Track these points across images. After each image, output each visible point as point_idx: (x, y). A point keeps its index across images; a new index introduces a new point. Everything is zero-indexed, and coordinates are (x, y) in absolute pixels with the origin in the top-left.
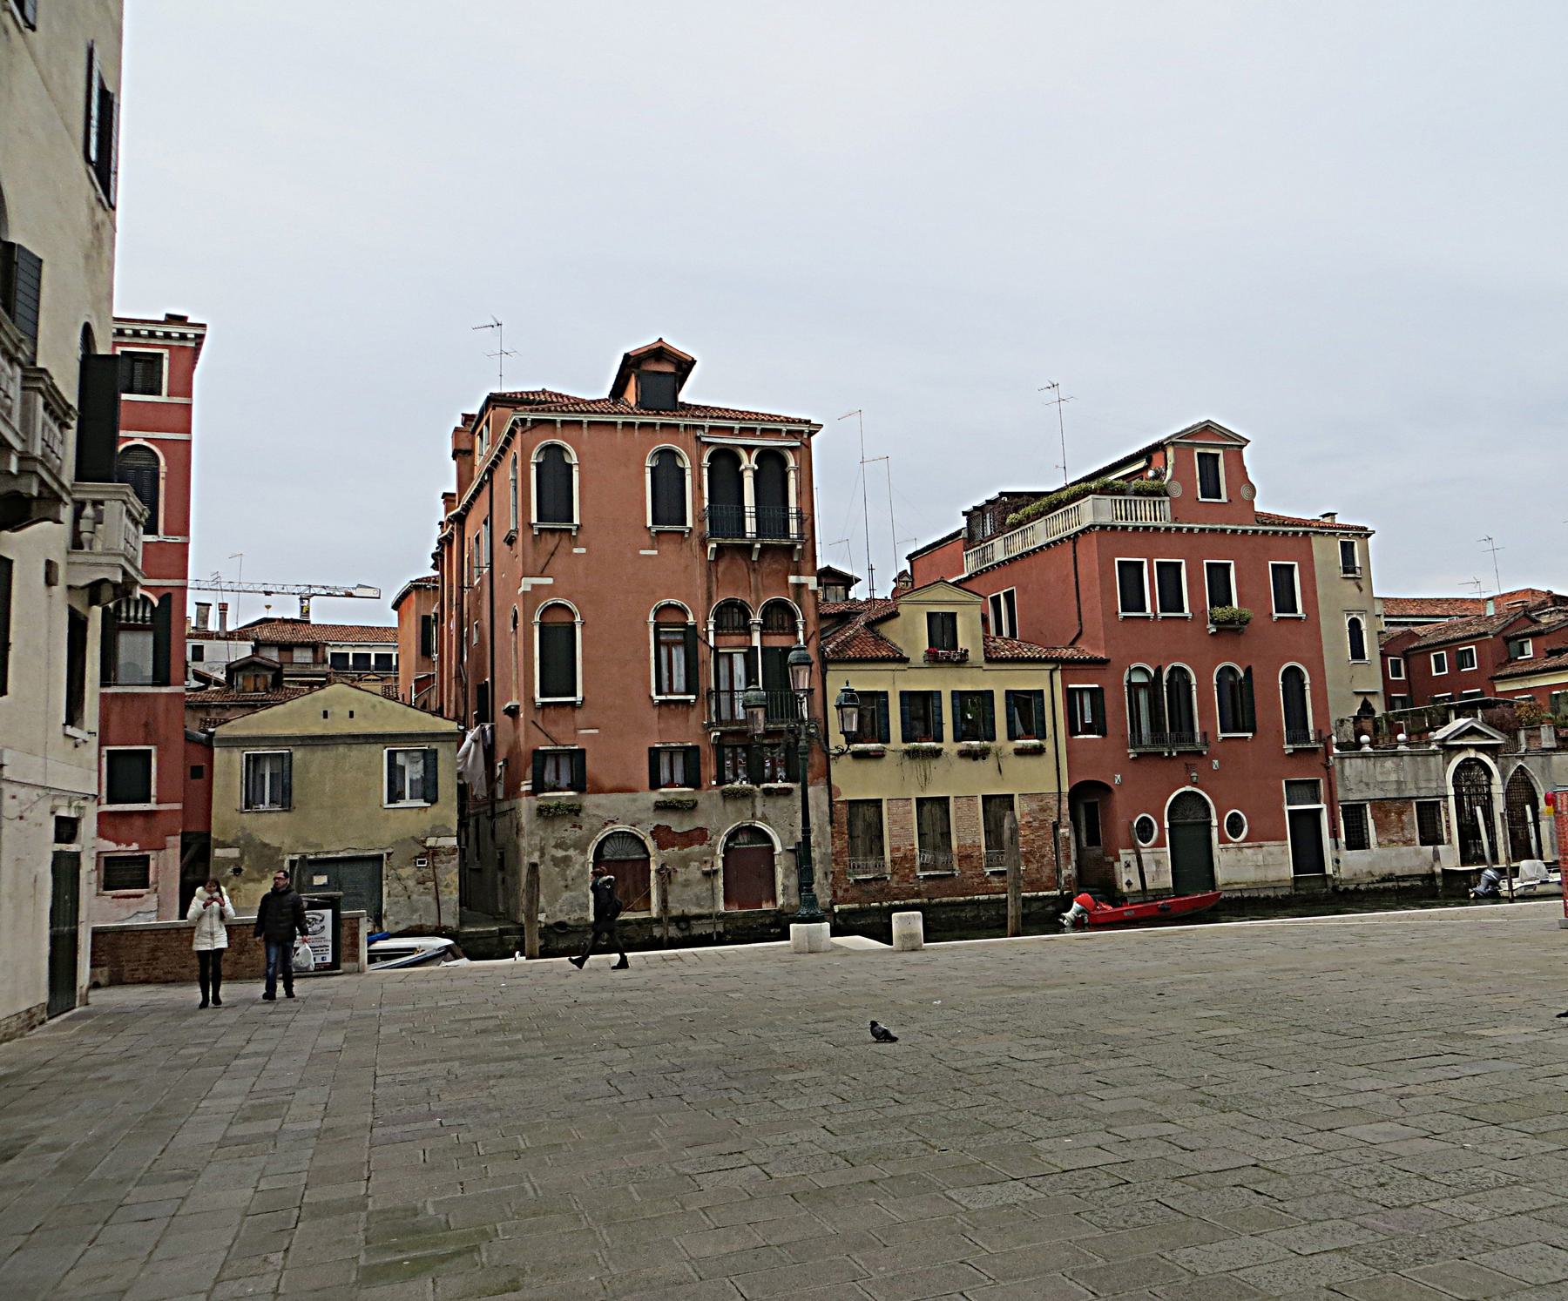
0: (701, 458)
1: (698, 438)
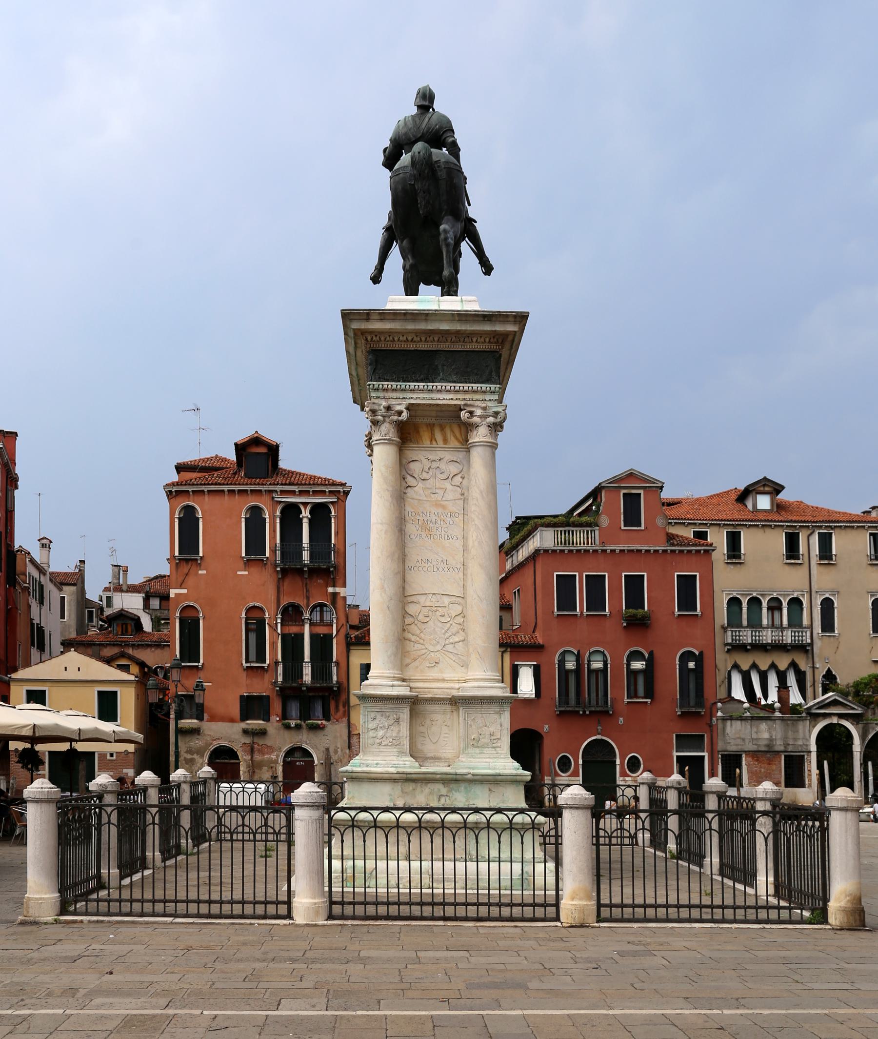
0: (274, 512)
1: (273, 498)
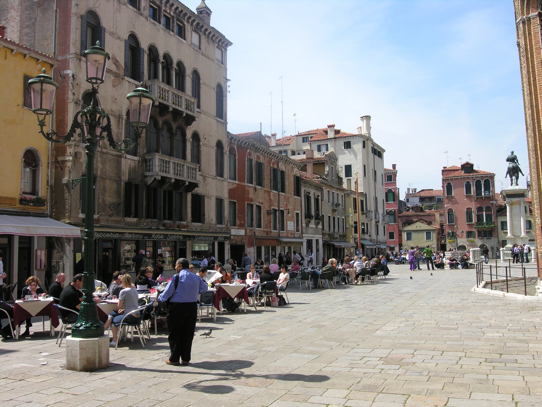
0: (473, 182)
